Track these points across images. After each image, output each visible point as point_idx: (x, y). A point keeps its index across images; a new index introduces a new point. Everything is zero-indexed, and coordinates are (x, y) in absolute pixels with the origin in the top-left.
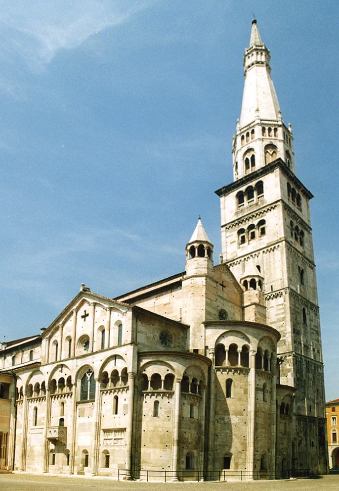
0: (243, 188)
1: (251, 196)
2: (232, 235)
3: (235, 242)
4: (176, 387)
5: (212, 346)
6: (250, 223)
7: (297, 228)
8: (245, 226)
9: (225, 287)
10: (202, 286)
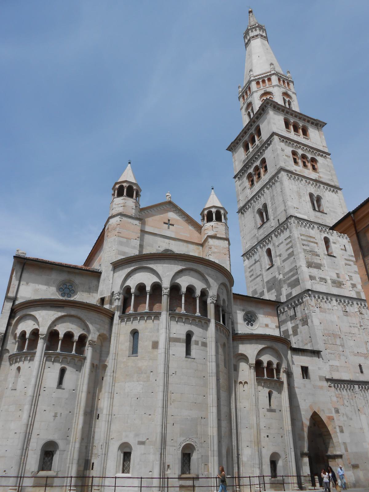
0: (246, 138)
1: (253, 141)
2: (243, 182)
3: (245, 187)
4: (41, 345)
5: (117, 289)
6: (255, 165)
7: (304, 157)
8: (251, 170)
9: (173, 225)
10: (116, 226)
